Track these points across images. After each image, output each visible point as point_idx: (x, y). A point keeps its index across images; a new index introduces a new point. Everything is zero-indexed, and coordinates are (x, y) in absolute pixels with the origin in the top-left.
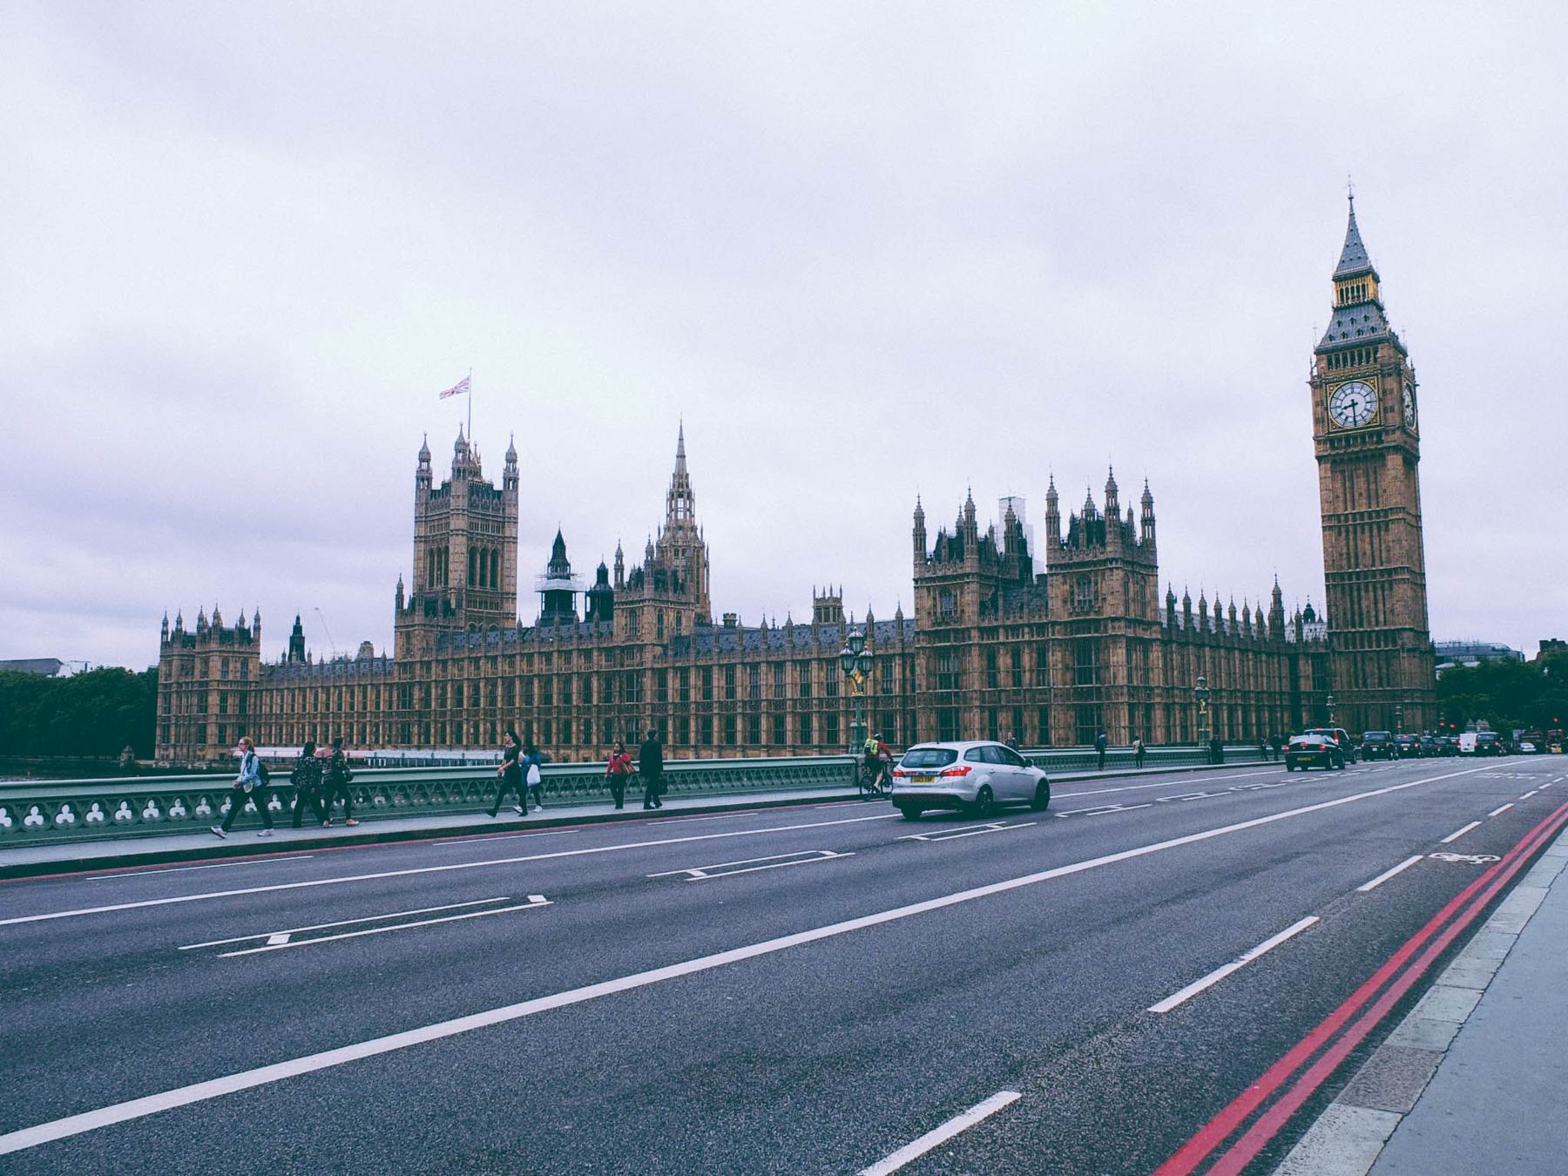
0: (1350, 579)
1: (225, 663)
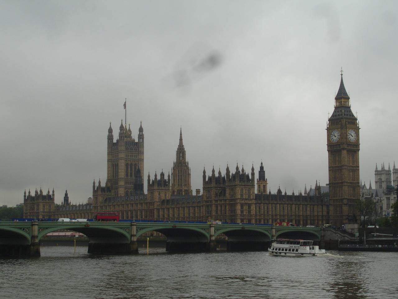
0: (334, 184)
1: (44, 206)
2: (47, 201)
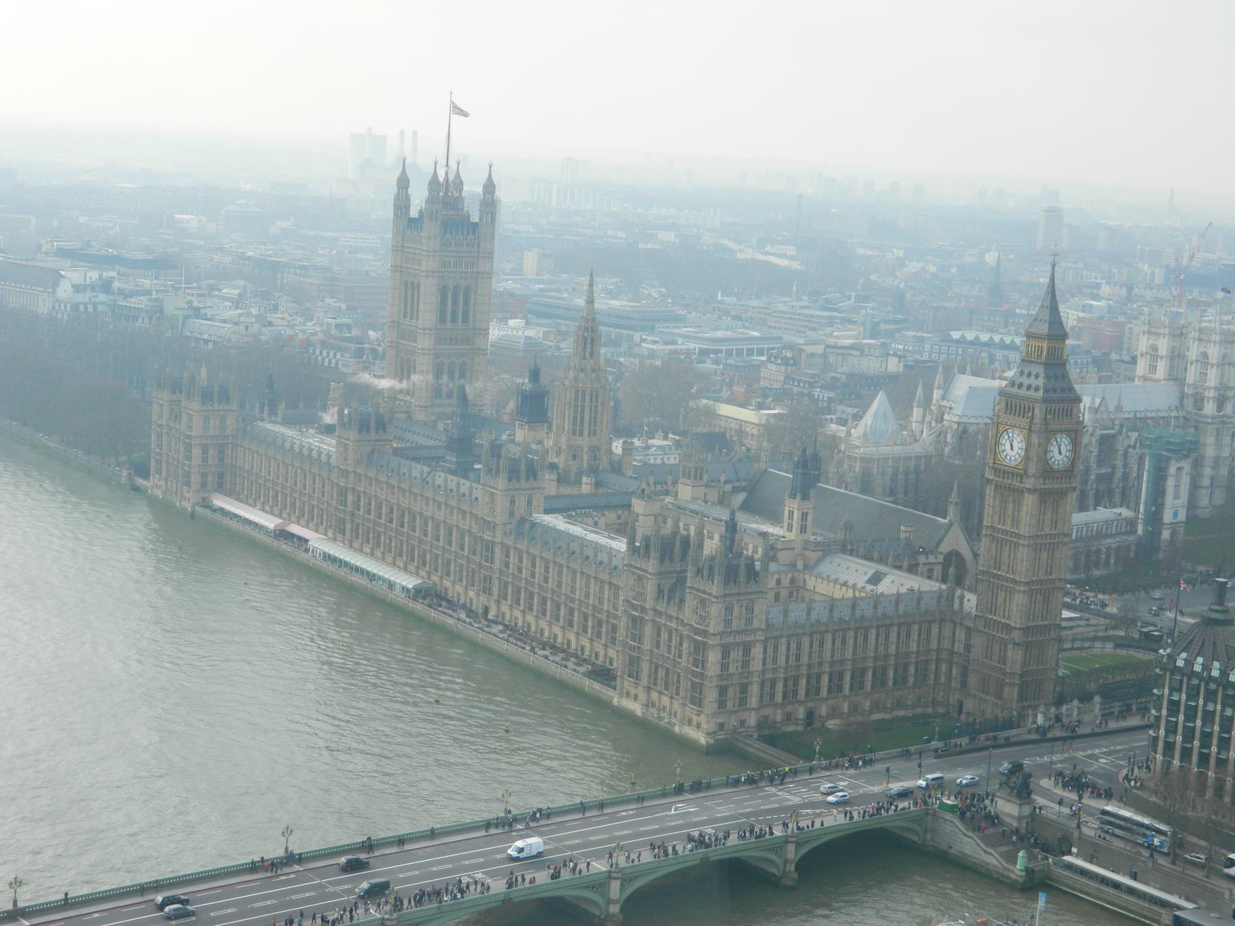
1: (206, 420)
2: (216, 407)
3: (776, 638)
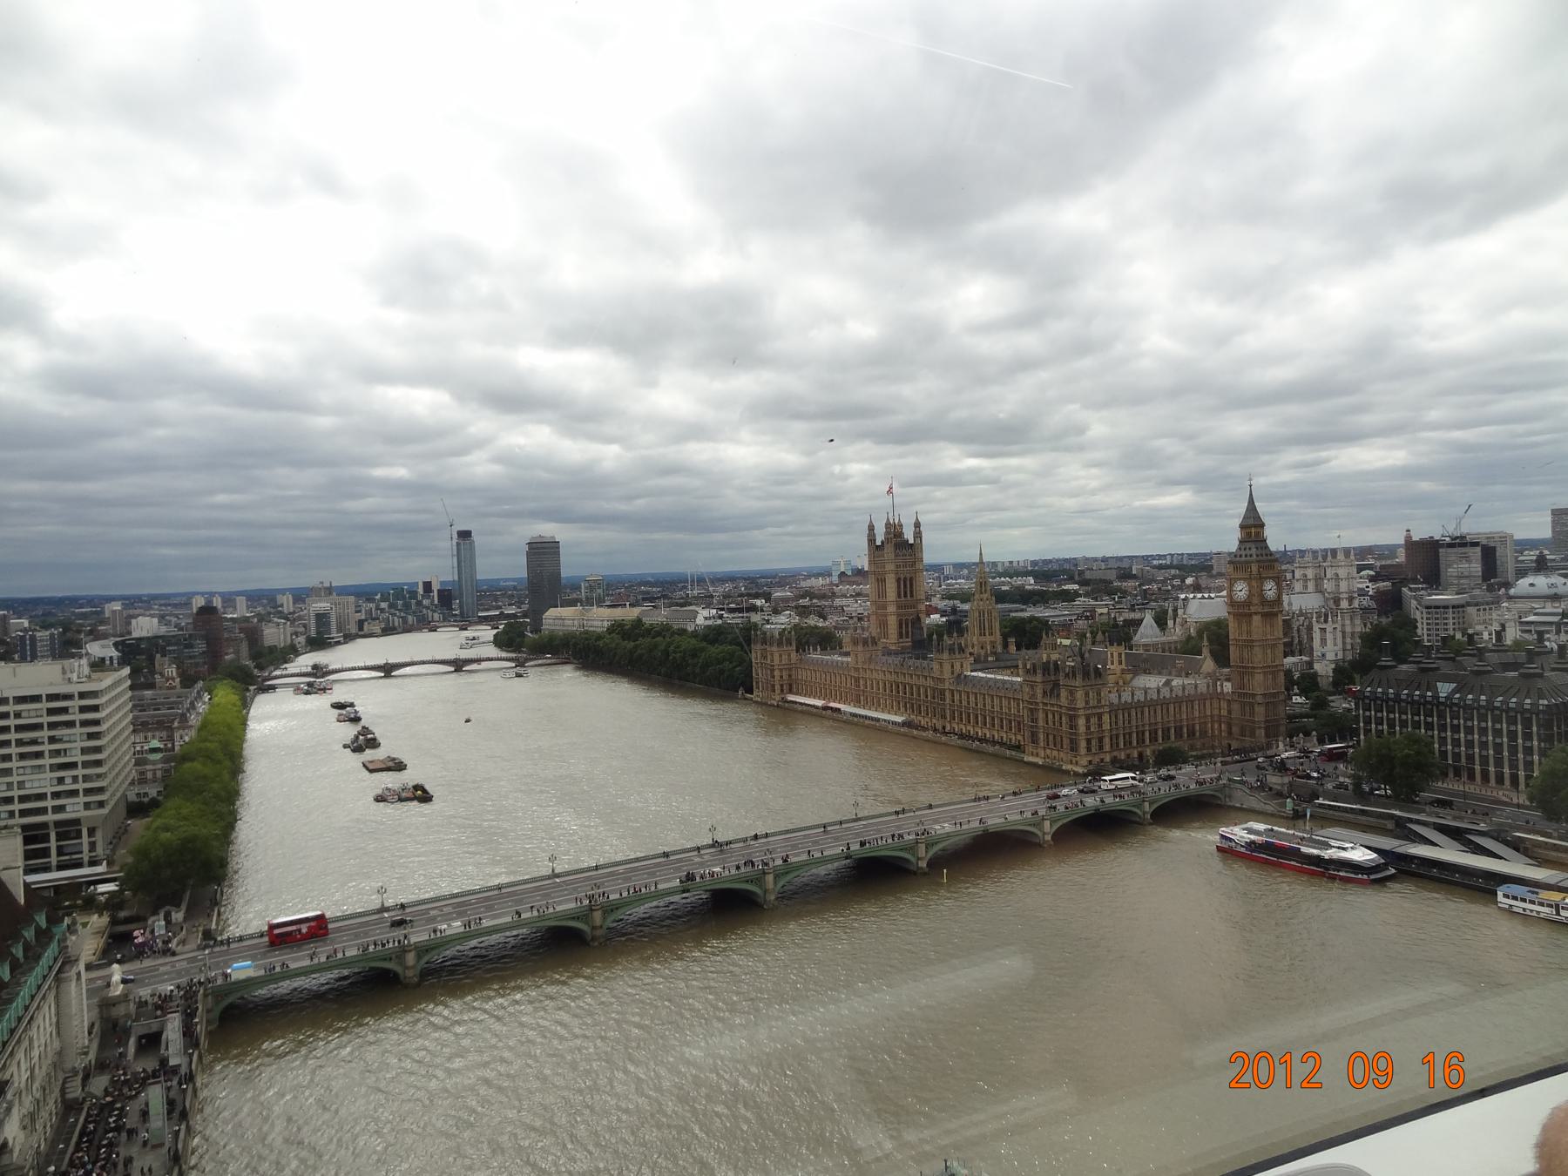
1: (781, 656)
3: (1116, 711)
